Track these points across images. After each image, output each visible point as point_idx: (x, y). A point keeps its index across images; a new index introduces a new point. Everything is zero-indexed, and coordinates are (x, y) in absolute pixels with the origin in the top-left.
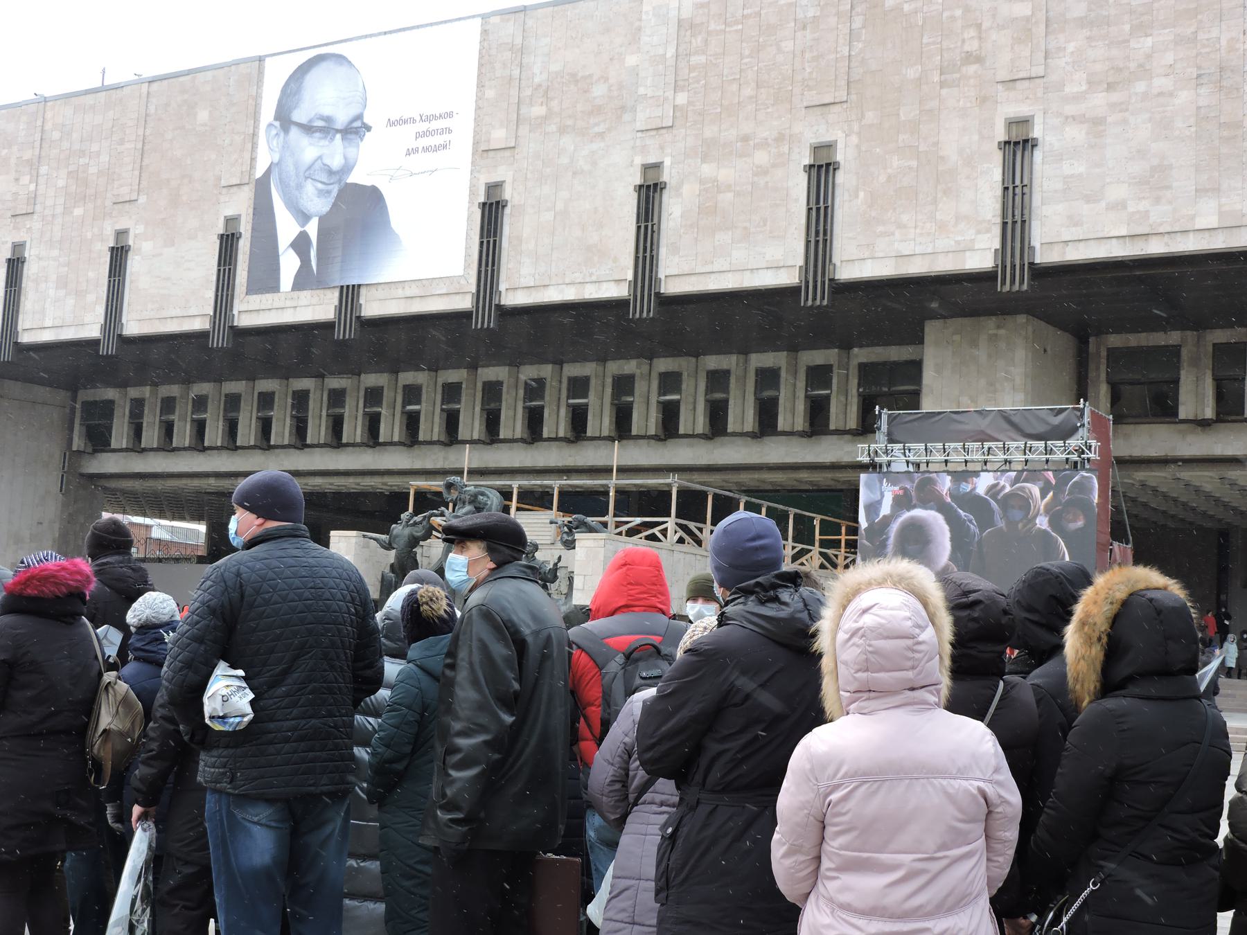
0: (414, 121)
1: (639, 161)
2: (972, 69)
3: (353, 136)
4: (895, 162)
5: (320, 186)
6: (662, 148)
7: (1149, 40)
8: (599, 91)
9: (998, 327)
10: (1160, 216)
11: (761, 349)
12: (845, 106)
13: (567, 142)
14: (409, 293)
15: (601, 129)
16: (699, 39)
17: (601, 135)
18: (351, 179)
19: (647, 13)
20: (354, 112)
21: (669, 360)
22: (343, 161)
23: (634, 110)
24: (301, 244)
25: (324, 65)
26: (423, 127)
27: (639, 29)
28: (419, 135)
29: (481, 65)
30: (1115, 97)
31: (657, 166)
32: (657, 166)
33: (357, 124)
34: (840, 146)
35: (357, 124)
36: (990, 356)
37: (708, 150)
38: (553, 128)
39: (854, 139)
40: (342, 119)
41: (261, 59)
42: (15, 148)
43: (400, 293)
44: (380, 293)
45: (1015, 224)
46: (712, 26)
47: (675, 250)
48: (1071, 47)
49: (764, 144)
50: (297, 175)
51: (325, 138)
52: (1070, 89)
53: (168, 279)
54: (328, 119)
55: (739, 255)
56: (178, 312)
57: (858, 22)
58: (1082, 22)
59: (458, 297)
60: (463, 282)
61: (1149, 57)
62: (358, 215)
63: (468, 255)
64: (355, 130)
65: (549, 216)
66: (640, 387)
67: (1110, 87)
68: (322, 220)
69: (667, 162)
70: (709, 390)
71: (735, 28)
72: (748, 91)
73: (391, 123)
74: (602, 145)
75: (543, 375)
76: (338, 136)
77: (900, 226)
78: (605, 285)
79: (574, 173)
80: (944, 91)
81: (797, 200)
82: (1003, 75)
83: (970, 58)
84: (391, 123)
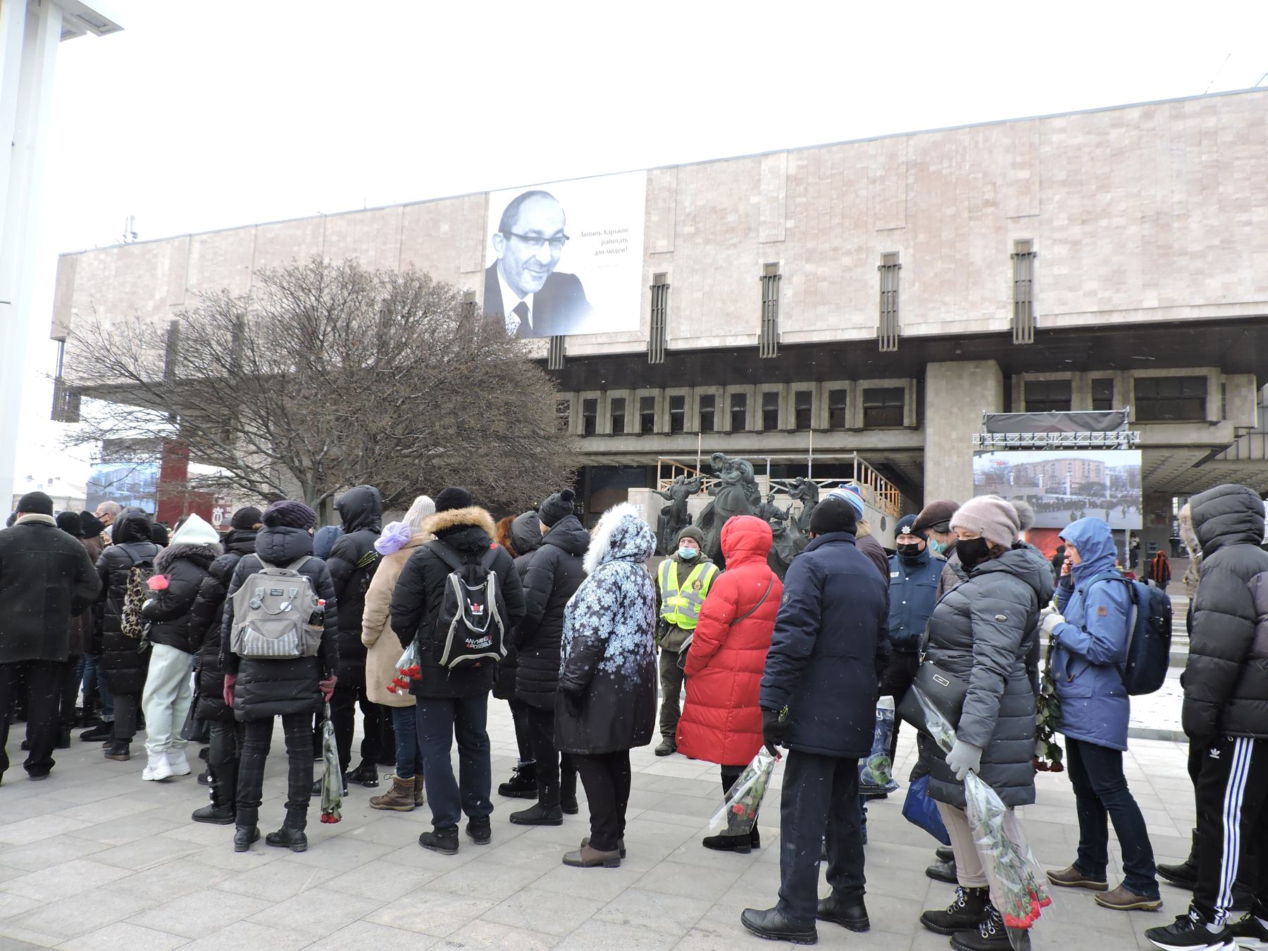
1: (761, 261)
2: (990, 210)
4: (939, 265)
6: (777, 254)
7: (1109, 196)
8: (732, 218)
10: (1119, 300)
13: (710, 249)
14: (600, 341)
15: (734, 241)
17: (734, 245)
18: (556, 269)
23: (757, 230)
24: (521, 310)
25: (534, 198)
26: (608, 237)
27: (759, 180)
29: (647, 201)
30: (1087, 228)
31: (775, 265)
32: (775, 265)
34: (901, 254)
37: (810, 256)
38: (700, 240)
39: (911, 251)
40: (548, 233)
41: (487, 193)
42: (304, 247)
43: (594, 341)
44: (579, 341)
45: (769, 321)
46: (810, 180)
47: (789, 316)
48: (1057, 198)
49: (848, 253)
52: (1055, 223)
54: (539, 233)
55: (833, 320)
57: (911, 180)
58: (1064, 183)
61: (1109, 205)
62: (561, 291)
63: (642, 318)
64: (558, 239)
65: (699, 295)
66: (719, 403)
67: (1084, 222)
68: (536, 295)
69: (782, 263)
70: (764, 404)
72: (836, 220)
73: (583, 235)
77: (945, 304)
82: (1011, 214)
83: (988, 203)
84: (583, 235)
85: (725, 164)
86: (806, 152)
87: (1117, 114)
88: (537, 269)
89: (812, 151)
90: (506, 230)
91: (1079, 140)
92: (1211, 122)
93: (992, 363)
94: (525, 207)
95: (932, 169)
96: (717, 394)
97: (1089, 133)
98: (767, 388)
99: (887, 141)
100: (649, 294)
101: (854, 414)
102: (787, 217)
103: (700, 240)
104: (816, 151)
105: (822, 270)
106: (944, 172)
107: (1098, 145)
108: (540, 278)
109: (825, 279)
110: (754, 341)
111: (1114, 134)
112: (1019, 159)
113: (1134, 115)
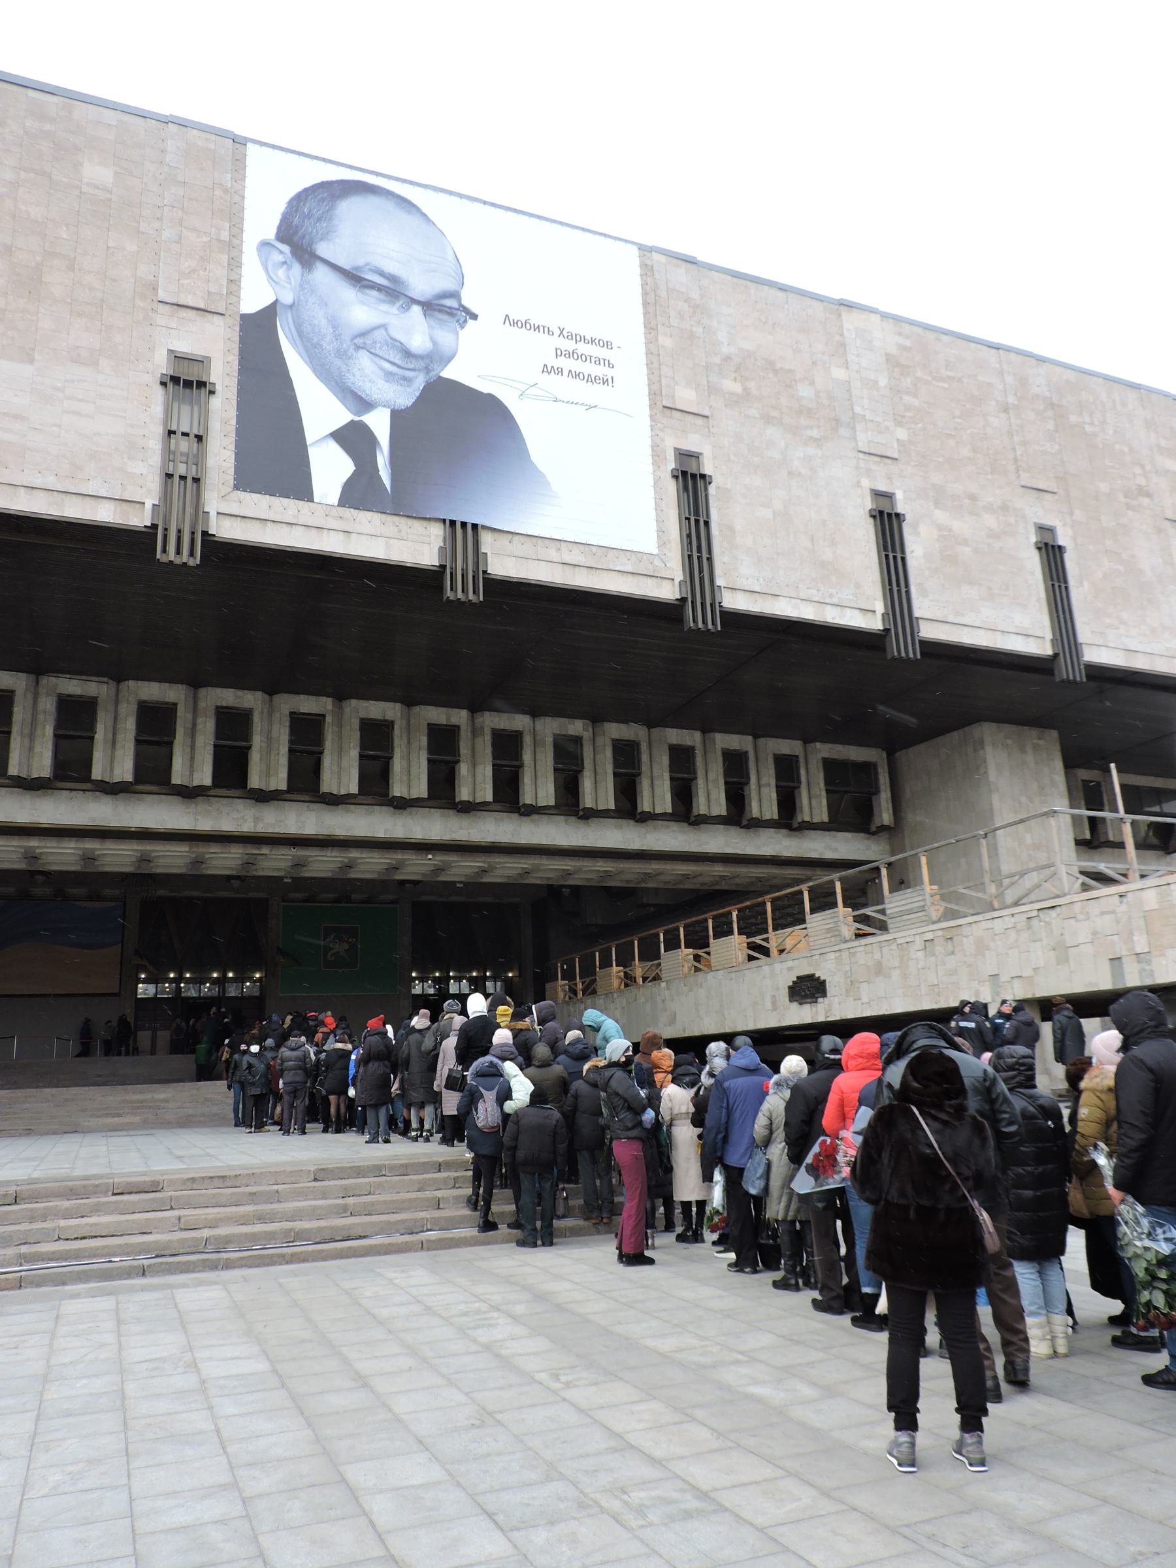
1: (866, 484)
2: (1146, 501)
3: (445, 317)
5: (387, 366)
8: (804, 391)
9: (1040, 738)
11: (726, 730)
12: (1056, 497)
13: (772, 432)
14: (568, 559)
15: (814, 433)
16: (909, 380)
17: (816, 440)
18: (448, 373)
19: (848, 330)
20: (449, 285)
21: (623, 726)
22: (429, 346)
26: (569, 345)
27: (843, 345)
28: (558, 353)
29: (645, 304)
32: (889, 496)
33: (450, 302)
35: (450, 302)
36: (1037, 763)
39: (1070, 532)
40: (422, 285)
41: (240, 142)
43: (553, 554)
44: (517, 546)
46: (919, 374)
47: (924, 593)
49: (989, 509)
50: (337, 337)
51: (393, 303)
53: (17, 417)
54: (393, 278)
55: (987, 614)
56: (51, 482)
57: (1051, 425)
59: (650, 581)
60: (657, 562)
62: (454, 429)
63: (661, 531)
68: (397, 417)
69: (899, 496)
71: (941, 384)
74: (820, 453)
75: (454, 721)
76: (416, 309)
78: (848, 612)
79: (790, 473)
80: (1130, 513)
81: (1032, 573)
83: (1144, 492)
85: (780, 294)
86: (907, 329)
89: (915, 328)
90: (298, 236)
93: (1054, 734)
94: (349, 209)
95: (1073, 418)
96: (587, 735)
98: (675, 736)
99: (1013, 356)
100: (671, 487)
101: (814, 803)
102: (899, 424)
103: (753, 412)
104: (920, 331)
106: (1088, 428)
108: (407, 381)
109: (965, 542)
110: (875, 624)
112: (1163, 443)
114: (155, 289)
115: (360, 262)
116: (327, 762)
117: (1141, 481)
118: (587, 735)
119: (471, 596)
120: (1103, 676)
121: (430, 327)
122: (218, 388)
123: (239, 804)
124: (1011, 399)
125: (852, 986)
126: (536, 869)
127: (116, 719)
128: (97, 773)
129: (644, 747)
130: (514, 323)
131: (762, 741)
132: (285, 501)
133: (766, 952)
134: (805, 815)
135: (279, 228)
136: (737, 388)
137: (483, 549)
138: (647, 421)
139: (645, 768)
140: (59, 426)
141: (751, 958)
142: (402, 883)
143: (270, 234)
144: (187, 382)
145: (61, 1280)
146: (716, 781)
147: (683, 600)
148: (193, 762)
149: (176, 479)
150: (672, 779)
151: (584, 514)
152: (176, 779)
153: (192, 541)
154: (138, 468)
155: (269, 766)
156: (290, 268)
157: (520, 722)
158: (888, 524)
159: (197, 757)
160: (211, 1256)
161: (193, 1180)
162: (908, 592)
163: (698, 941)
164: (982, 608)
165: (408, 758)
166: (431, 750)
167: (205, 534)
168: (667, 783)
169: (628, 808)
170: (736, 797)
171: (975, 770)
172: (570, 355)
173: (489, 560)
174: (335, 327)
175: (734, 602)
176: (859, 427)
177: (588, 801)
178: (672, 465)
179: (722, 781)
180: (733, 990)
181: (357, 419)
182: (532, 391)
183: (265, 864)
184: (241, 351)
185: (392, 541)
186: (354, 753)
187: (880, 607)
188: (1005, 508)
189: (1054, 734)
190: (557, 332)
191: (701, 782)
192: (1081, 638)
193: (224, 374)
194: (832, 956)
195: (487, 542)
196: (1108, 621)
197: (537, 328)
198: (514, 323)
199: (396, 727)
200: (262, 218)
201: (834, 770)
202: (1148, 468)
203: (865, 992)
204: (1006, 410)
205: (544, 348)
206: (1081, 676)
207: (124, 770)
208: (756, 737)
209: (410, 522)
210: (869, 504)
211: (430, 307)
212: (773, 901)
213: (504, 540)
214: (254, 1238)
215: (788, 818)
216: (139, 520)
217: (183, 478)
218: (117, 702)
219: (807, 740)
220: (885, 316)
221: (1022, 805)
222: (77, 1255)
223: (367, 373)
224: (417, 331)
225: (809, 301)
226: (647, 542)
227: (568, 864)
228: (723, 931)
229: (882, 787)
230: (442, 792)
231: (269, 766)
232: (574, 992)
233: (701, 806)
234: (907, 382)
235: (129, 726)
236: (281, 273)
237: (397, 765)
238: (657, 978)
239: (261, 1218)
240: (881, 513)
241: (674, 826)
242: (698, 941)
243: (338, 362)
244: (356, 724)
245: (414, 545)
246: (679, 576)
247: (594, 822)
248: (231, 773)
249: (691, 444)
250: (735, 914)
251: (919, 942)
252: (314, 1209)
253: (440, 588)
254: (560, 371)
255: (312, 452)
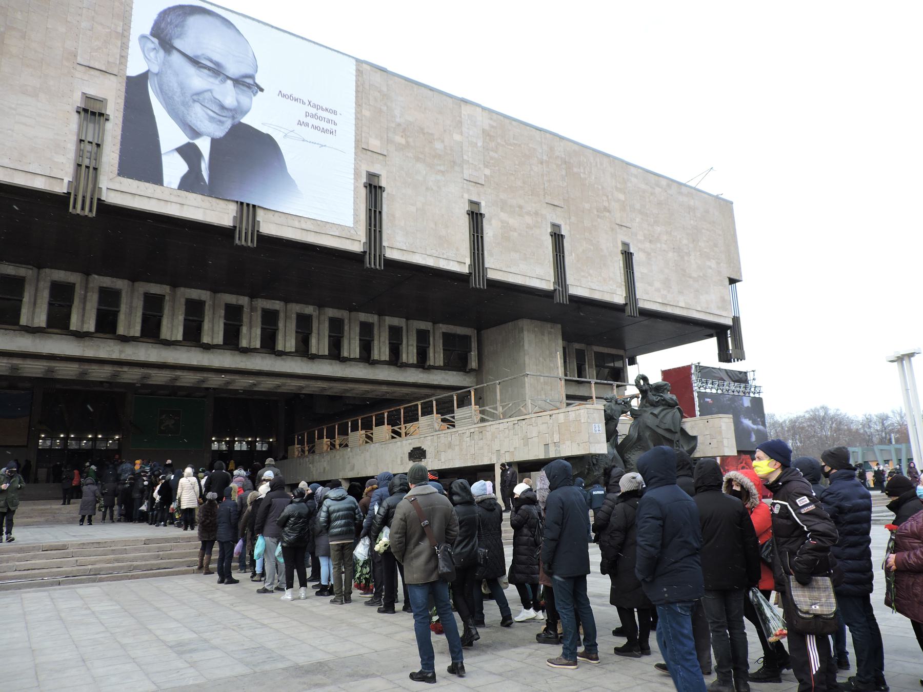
0: (304, 103)
1: (466, 196)
2: (607, 214)
3: (245, 88)
8: (438, 146)
13: (420, 166)
14: (304, 226)
15: (442, 168)
17: (442, 172)
18: (246, 120)
20: (249, 71)
21: (335, 310)
22: (235, 103)
25: (209, 19)
26: (314, 111)
27: (461, 122)
28: (307, 114)
29: (357, 91)
32: (478, 204)
37: (504, 206)
40: (233, 69)
43: (297, 224)
44: (276, 218)
46: (499, 141)
47: (491, 255)
49: (528, 213)
50: (183, 94)
54: (217, 64)
55: (523, 267)
57: (564, 173)
59: (348, 241)
60: (352, 231)
62: (244, 152)
67: (650, 242)
68: (215, 143)
69: (483, 204)
72: (519, 183)
75: (240, 302)
76: (229, 82)
77: (590, 275)
79: (427, 189)
83: (607, 210)
85: (430, 92)
86: (495, 116)
87: (657, 178)
88: (217, 109)
91: (643, 186)
92: (692, 203)
93: (559, 326)
94: (194, 21)
96: (315, 314)
97: (647, 184)
98: (363, 317)
100: (363, 192)
101: (436, 356)
102: (486, 166)
103: (410, 155)
104: (502, 118)
105: (513, 221)
107: (652, 194)
108: (222, 122)
109: (515, 230)
110: (465, 270)
111: (658, 190)
112: (619, 186)
113: (664, 183)
114: (75, 56)
115: (199, 53)
116: (165, 322)
117: (606, 204)
118: (315, 314)
119: (249, 244)
120: (580, 302)
121: (237, 93)
122: (111, 117)
123: (111, 343)
124: (545, 158)
125: (438, 452)
126: (284, 385)
127: (36, 290)
128: (23, 321)
129: (346, 321)
130: (284, 96)
131: (411, 322)
132: (147, 184)
133: (399, 434)
134: (431, 362)
135: (153, 29)
136: (403, 141)
137: (258, 219)
138: (353, 156)
139: (346, 334)
140: (13, 131)
141: (393, 437)
142: (207, 389)
143: (147, 31)
144: (92, 112)
145: (19, 587)
146: (384, 342)
147: (365, 252)
148: (84, 317)
149: (83, 168)
150: (360, 340)
151: (315, 203)
152: (73, 327)
153: (91, 203)
154: (60, 159)
155: (130, 321)
156: (157, 52)
157: (277, 305)
158: (476, 218)
159: (86, 315)
160: (94, 576)
161: (83, 544)
162: (483, 254)
163: (367, 426)
164: (520, 263)
165: (212, 321)
166: (226, 317)
167: (99, 200)
168: (358, 342)
169: (335, 354)
170: (395, 351)
171: (519, 344)
172: (313, 116)
173: (261, 224)
174: (182, 89)
175: (392, 254)
176: (465, 166)
177: (313, 350)
178: (364, 180)
179: (387, 342)
180: (381, 454)
181: (191, 141)
182: (292, 134)
183: (125, 376)
184: (126, 97)
185: (208, 211)
186: (181, 318)
187: (468, 261)
188: (536, 213)
189: (559, 326)
190: (307, 103)
191: (376, 342)
192: (568, 282)
193: (115, 110)
194: (429, 438)
195: (261, 216)
196: (583, 274)
197: (296, 100)
198: (284, 96)
199: (207, 305)
200: (142, 21)
201: (448, 339)
202: (610, 197)
203: (443, 457)
204: (542, 163)
205: (299, 111)
206: (566, 301)
207: (41, 320)
208: (407, 319)
209: (218, 201)
210: (467, 208)
211: (238, 82)
212: (405, 408)
213: (270, 214)
214: (114, 569)
215: (422, 363)
216: (61, 188)
217: (87, 167)
218: (38, 281)
219: (435, 322)
220: (484, 109)
221: (541, 363)
222: (26, 577)
223: (199, 116)
224: (229, 95)
225: (445, 97)
226: (348, 221)
227: (302, 383)
228: (380, 423)
229: (473, 349)
230: (232, 341)
231: (130, 321)
232: (303, 451)
233: (375, 356)
234: (493, 145)
235: (45, 295)
236: (152, 54)
237: (206, 326)
238: (347, 446)
239: (117, 560)
240: (473, 212)
241: (361, 365)
242: (367, 426)
243: (182, 108)
244: (183, 301)
245: (218, 213)
246: (363, 239)
247: (317, 361)
248: (107, 325)
249: (375, 169)
250: (386, 415)
251: (468, 434)
252: (143, 556)
253: (233, 237)
254: (307, 125)
255: (165, 159)
